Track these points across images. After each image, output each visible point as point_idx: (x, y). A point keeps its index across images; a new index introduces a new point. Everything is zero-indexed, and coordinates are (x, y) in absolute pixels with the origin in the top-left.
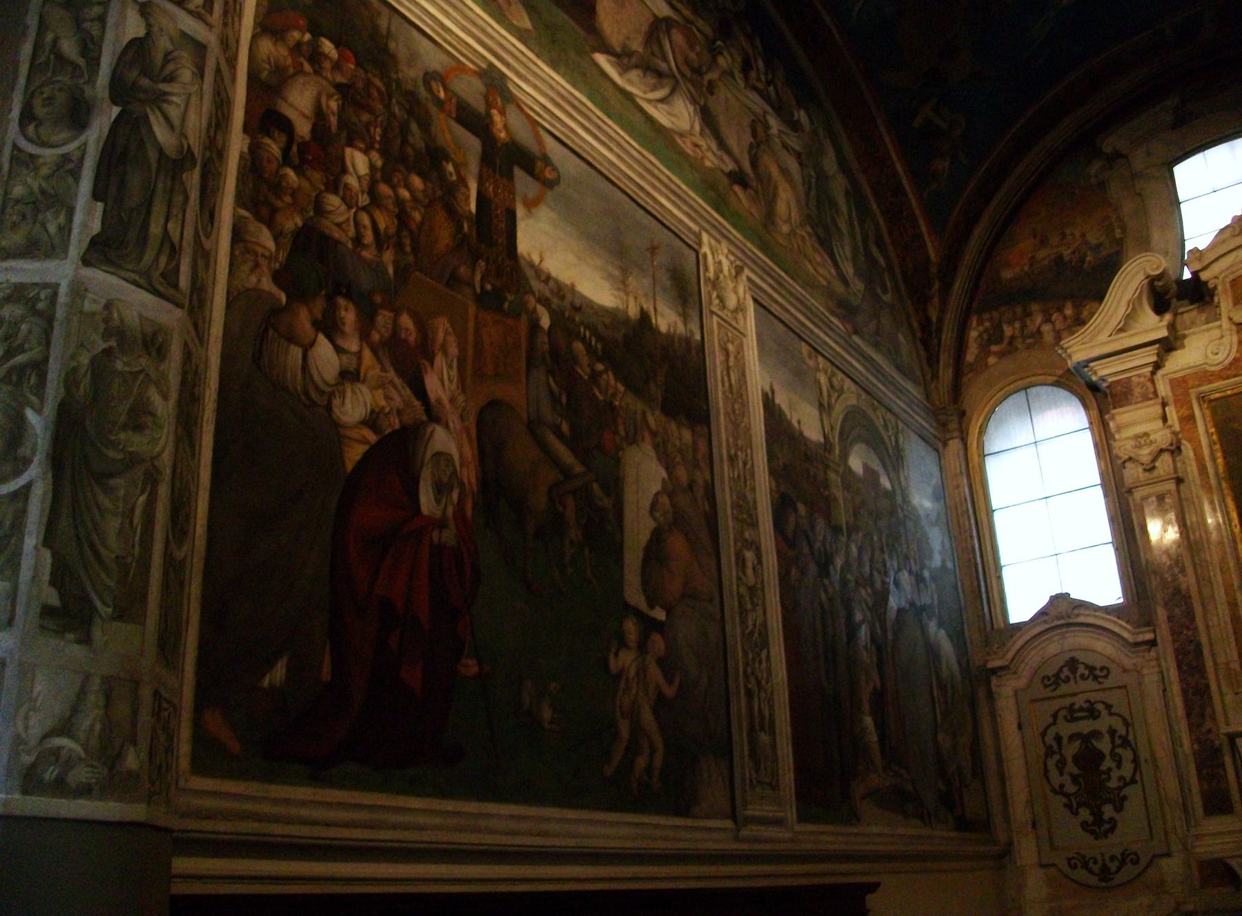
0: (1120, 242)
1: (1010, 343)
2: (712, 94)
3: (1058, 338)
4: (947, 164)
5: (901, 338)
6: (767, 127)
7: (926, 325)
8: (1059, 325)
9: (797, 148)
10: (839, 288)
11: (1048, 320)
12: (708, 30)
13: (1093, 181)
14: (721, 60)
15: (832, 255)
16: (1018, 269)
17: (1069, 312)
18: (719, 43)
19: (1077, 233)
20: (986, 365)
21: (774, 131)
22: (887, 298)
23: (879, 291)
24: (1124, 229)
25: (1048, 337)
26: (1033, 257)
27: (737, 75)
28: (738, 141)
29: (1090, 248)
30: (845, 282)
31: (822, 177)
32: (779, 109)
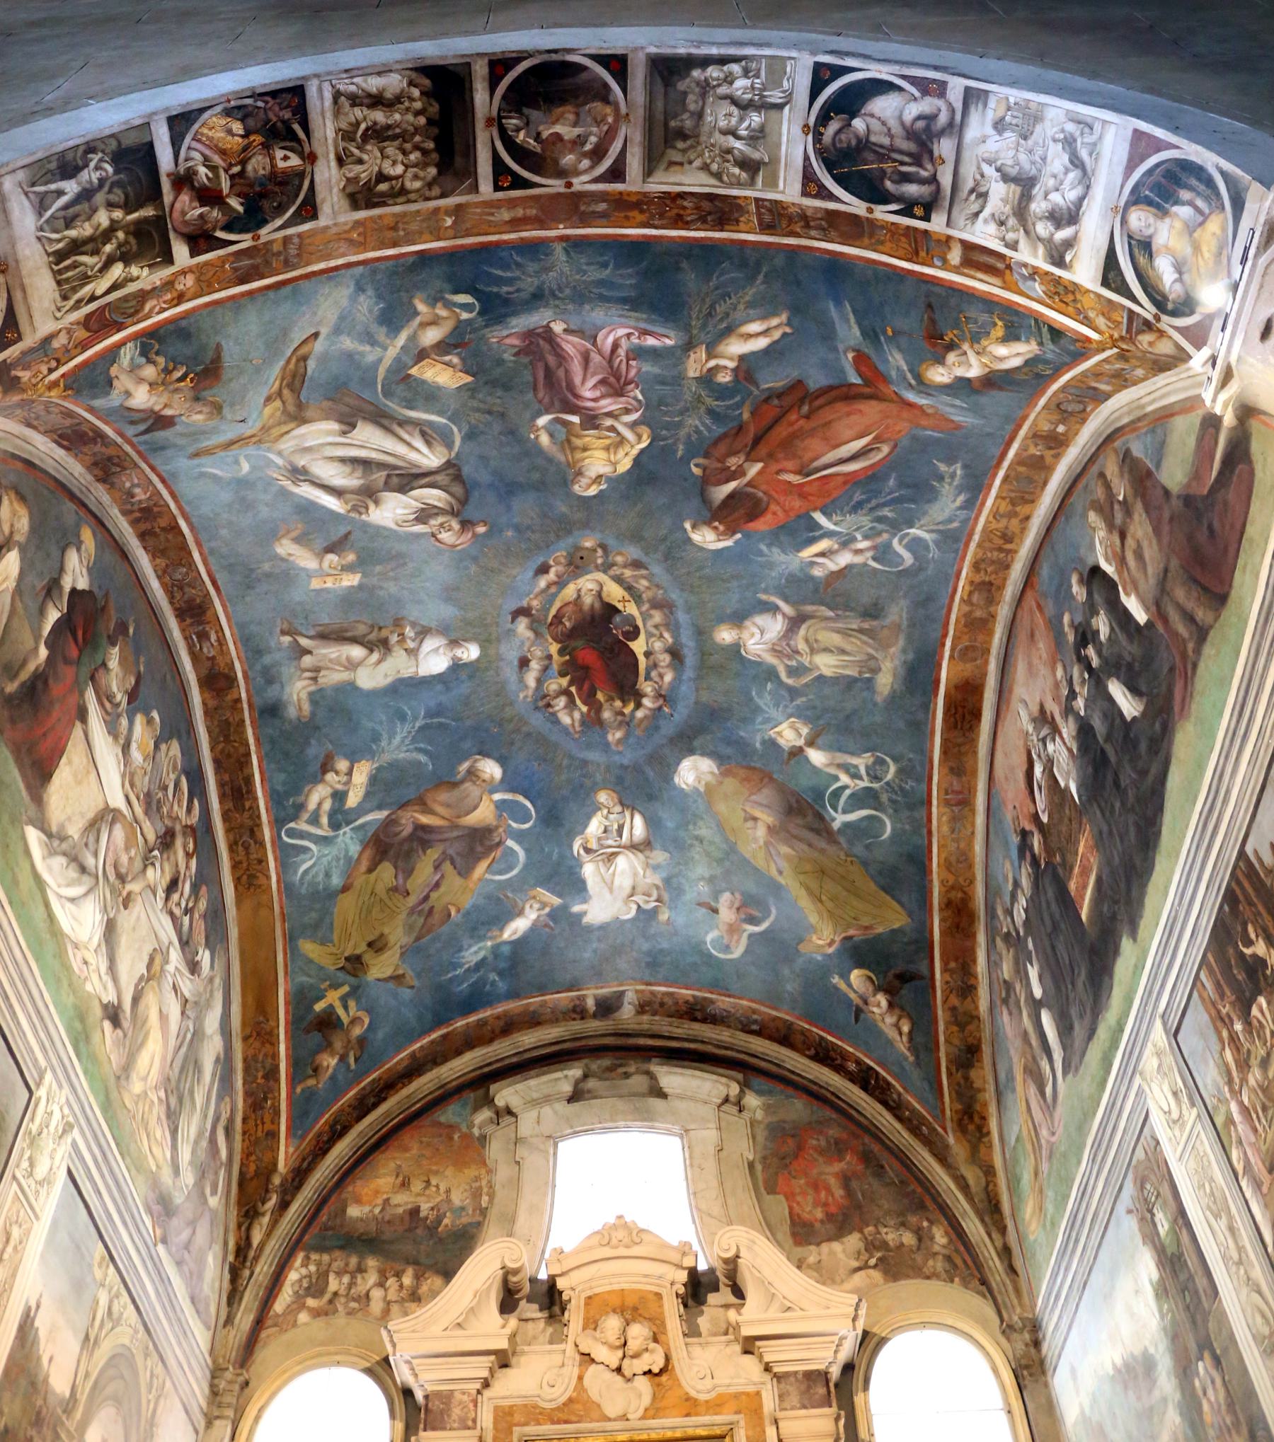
0: (484, 1212)
1: (331, 1302)
2: (126, 907)
3: (386, 1313)
4: (333, 1062)
5: (210, 1259)
6: (166, 961)
7: (242, 1251)
8: (392, 1295)
9: (187, 995)
10: (166, 1176)
11: (381, 1284)
12: (151, 837)
13: (476, 1132)
14: (150, 872)
15: (174, 1132)
16: (367, 1209)
17: (407, 1280)
18: (156, 853)
19: (442, 1188)
20: (295, 1325)
21: (170, 968)
22: (213, 1201)
23: (208, 1191)
24: (492, 1196)
25: (376, 1306)
26: (388, 1200)
27: (161, 894)
28: (131, 966)
29: (450, 1209)
30: (176, 1170)
31: (198, 1034)
32: (185, 943)
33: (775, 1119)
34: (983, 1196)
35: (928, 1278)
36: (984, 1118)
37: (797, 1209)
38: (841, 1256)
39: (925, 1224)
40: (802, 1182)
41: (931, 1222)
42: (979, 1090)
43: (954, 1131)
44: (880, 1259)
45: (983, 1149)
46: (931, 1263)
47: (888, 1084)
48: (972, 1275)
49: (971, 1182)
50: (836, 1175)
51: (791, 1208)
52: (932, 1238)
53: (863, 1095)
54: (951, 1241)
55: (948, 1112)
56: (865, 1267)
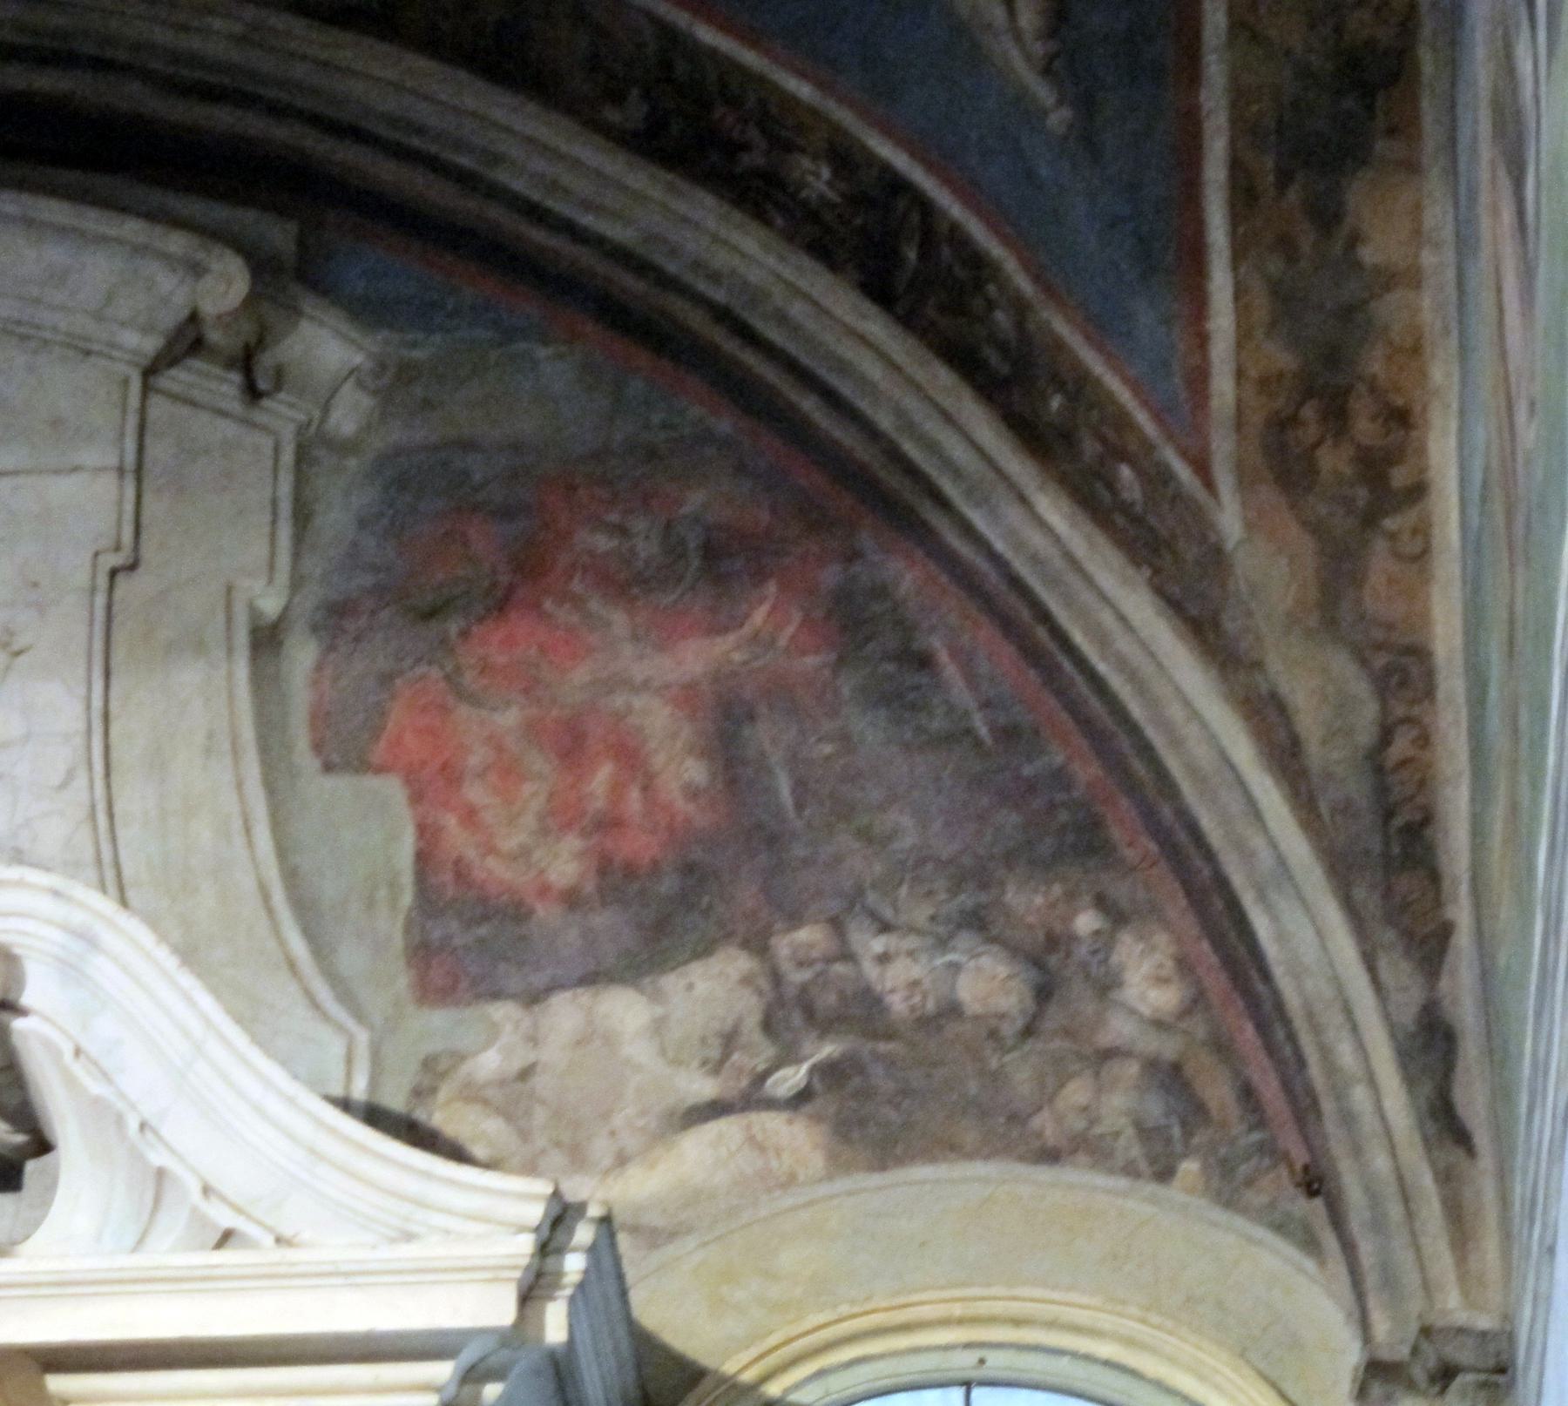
33: (421, 433)
34: (1357, 788)
35: (1050, 1156)
36: (1401, 418)
37: (457, 838)
38: (640, 1051)
39: (1087, 922)
40: (509, 718)
41: (1117, 916)
42: (1387, 279)
43: (1246, 481)
44: (832, 1073)
45: (1380, 563)
46: (1077, 1092)
47: (978, 262)
48: (1270, 1150)
49: (1309, 721)
50: (686, 697)
51: (427, 834)
52: (1106, 986)
53: (877, 326)
54: (1197, 1002)
55: (1223, 387)
56: (752, 1099)
